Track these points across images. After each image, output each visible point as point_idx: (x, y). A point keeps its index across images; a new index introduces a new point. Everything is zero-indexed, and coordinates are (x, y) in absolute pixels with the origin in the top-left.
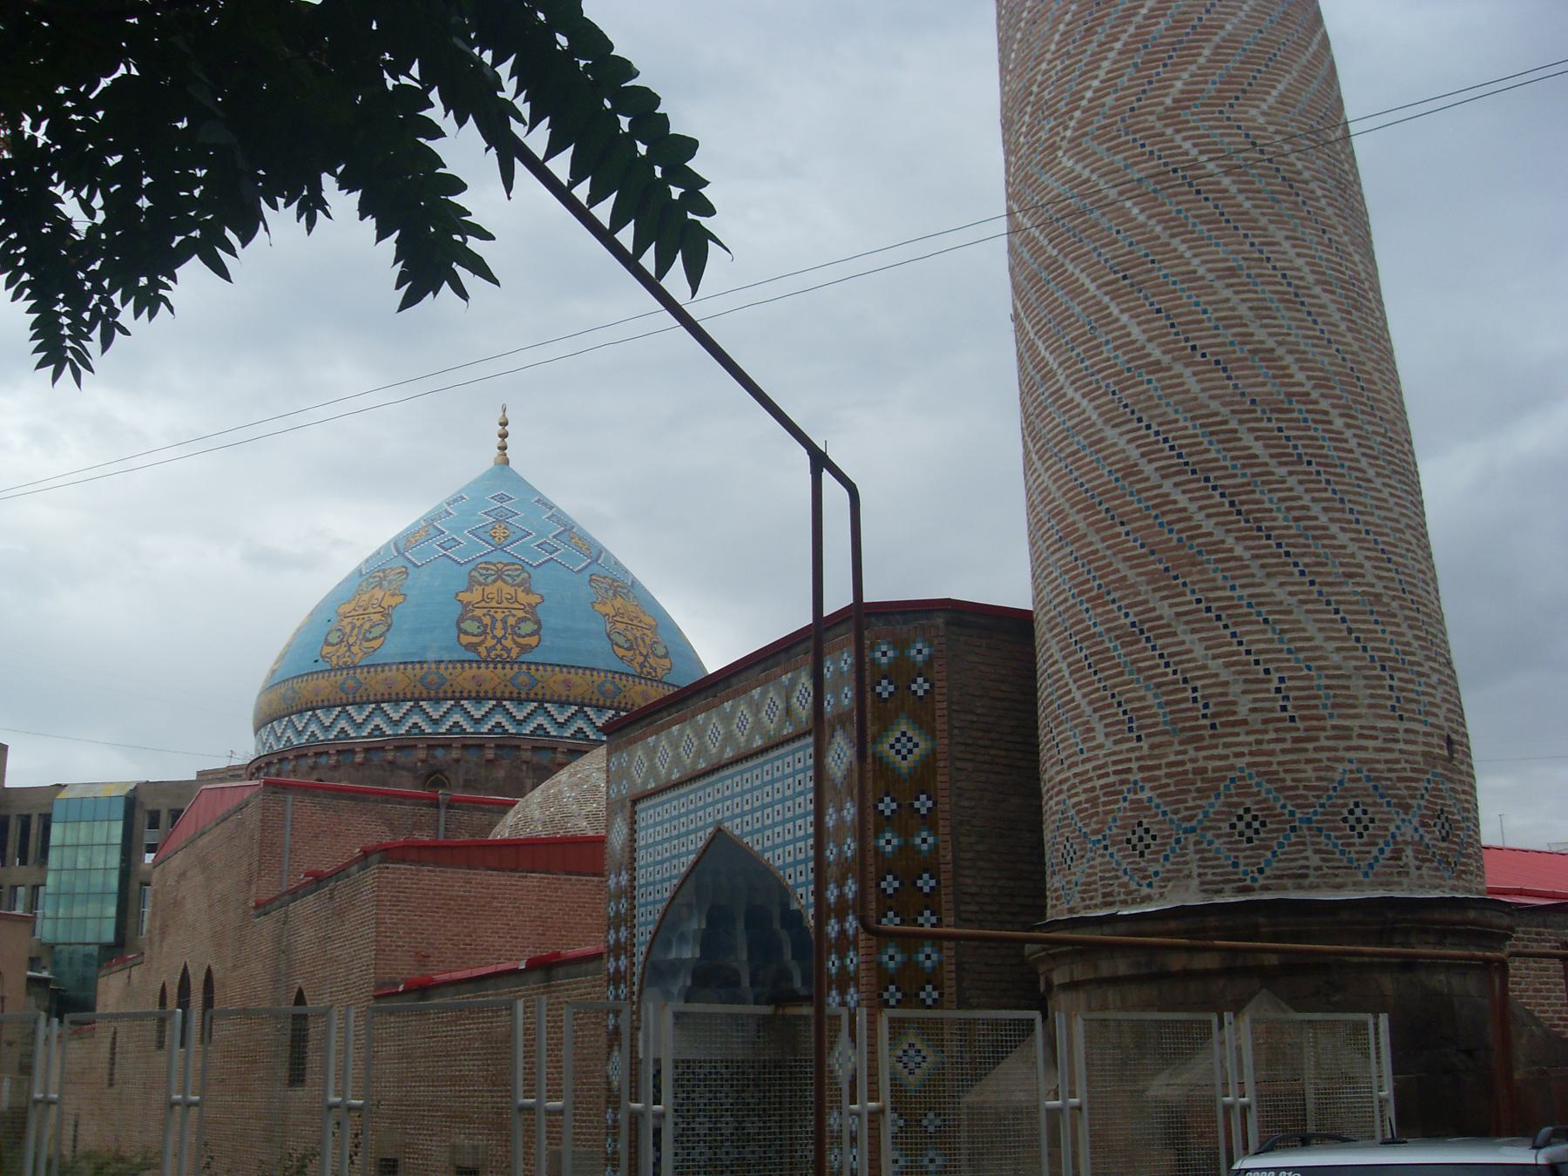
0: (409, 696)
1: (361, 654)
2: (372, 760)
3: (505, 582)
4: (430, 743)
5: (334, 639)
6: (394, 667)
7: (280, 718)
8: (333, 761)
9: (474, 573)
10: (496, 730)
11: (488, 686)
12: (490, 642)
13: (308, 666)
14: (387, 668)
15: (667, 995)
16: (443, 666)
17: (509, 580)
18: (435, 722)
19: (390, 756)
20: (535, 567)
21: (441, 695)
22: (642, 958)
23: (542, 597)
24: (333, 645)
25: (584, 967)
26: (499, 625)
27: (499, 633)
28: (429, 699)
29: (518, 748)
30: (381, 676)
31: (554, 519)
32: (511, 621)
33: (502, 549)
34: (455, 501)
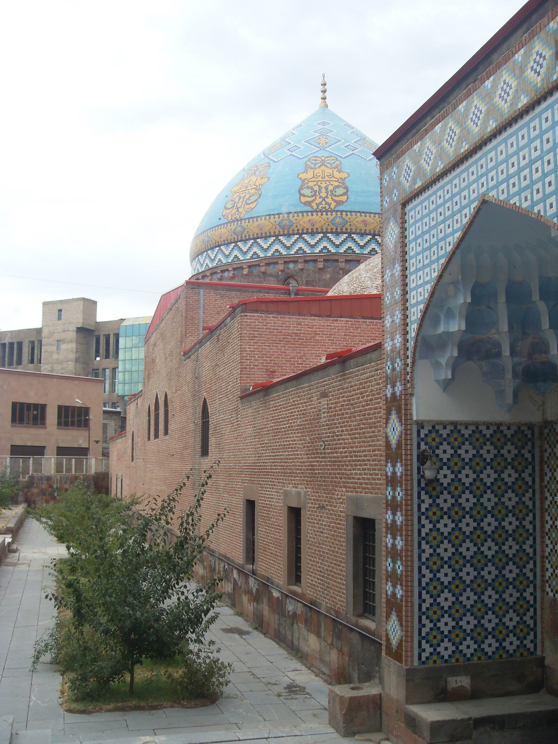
0: (272, 234)
1: (244, 213)
2: (252, 272)
3: (327, 167)
4: (286, 260)
5: (229, 205)
6: (263, 218)
7: (202, 253)
8: (231, 274)
9: (308, 163)
10: (324, 251)
11: (318, 225)
12: (318, 200)
13: (216, 222)
14: (259, 219)
15: (437, 365)
16: (291, 215)
17: (329, 165)
18: (288, 248)
19: (263, 269)
20: (344, 158)
21: (291, 232)
22: (413, 334)
23: (348, 174)
24: (229, 209)
25: (368, 356)
26: (323, 190)
27: (323, 195)
28: (284, 235)
29: (337, 261)
30: (256, 224)
31: (355, 133)
32: (330, 188)
33: (324, 149)
34: (297, 128)
